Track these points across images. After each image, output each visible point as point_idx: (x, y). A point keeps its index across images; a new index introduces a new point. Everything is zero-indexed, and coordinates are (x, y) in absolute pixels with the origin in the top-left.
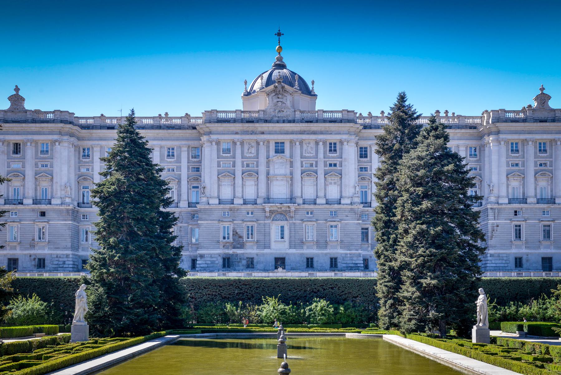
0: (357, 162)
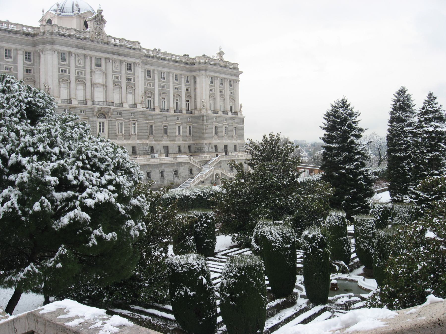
0: (143, 79)
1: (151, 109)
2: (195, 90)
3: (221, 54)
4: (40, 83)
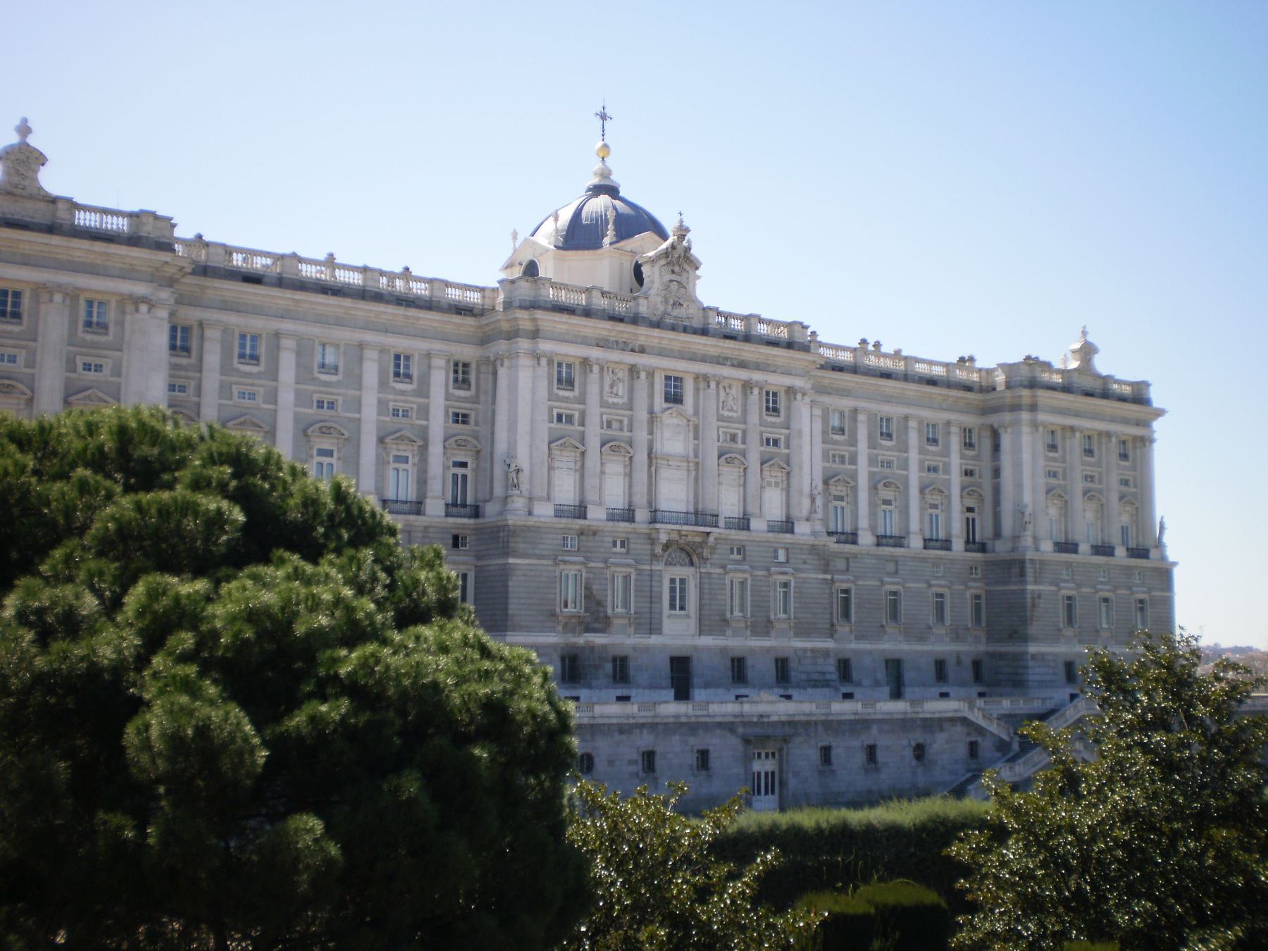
1: (843, 537)
2: (997, 472)
3: (1087, 351)
4: (492, 454)
